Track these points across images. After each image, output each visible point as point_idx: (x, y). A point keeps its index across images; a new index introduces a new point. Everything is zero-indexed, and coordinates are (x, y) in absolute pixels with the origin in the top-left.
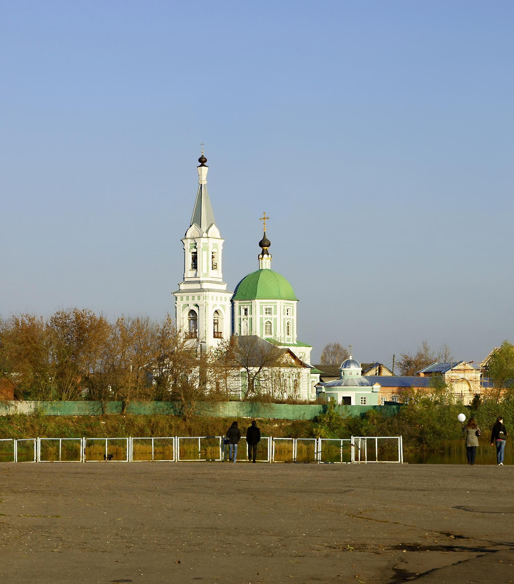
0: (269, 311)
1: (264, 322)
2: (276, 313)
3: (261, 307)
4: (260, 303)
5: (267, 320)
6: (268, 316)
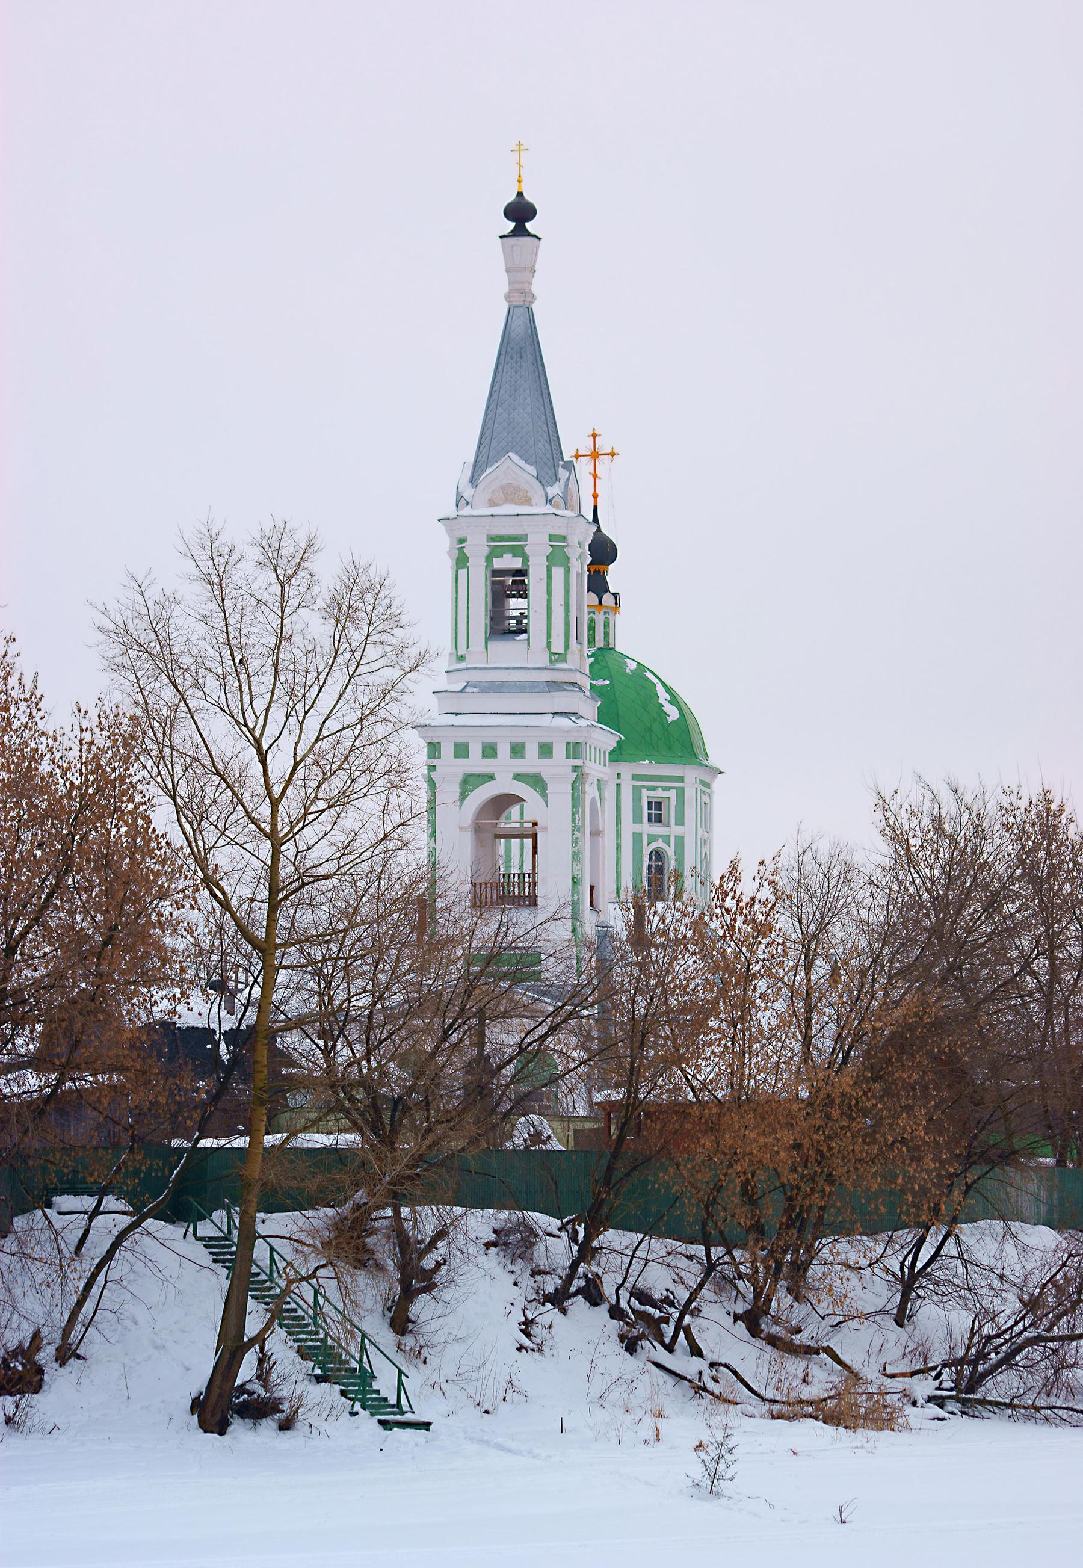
0: (657, 812)
1: (647, 850)
2: (680, 821)
4: (635, 777)
5: (654, 846)
6: (658, 830)
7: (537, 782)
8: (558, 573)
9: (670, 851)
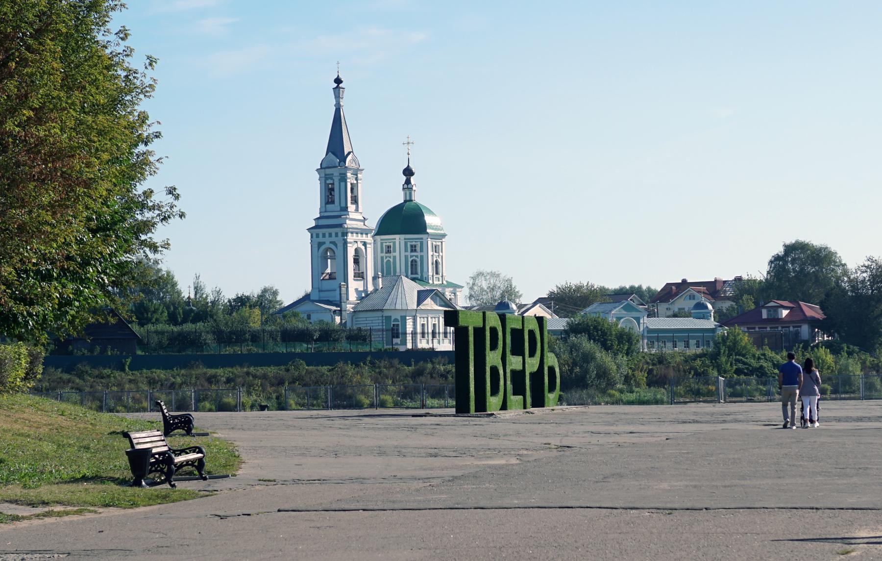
0: (413, 249)
1: (410, 260)
2: (422, 250)
3: (406, 244)
7: (334, 243)
8: (343, 184)
9: (418, 260)
